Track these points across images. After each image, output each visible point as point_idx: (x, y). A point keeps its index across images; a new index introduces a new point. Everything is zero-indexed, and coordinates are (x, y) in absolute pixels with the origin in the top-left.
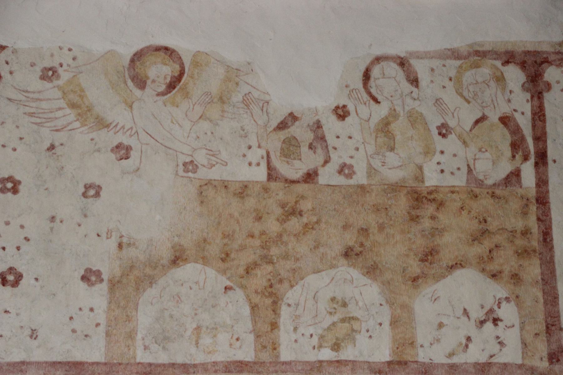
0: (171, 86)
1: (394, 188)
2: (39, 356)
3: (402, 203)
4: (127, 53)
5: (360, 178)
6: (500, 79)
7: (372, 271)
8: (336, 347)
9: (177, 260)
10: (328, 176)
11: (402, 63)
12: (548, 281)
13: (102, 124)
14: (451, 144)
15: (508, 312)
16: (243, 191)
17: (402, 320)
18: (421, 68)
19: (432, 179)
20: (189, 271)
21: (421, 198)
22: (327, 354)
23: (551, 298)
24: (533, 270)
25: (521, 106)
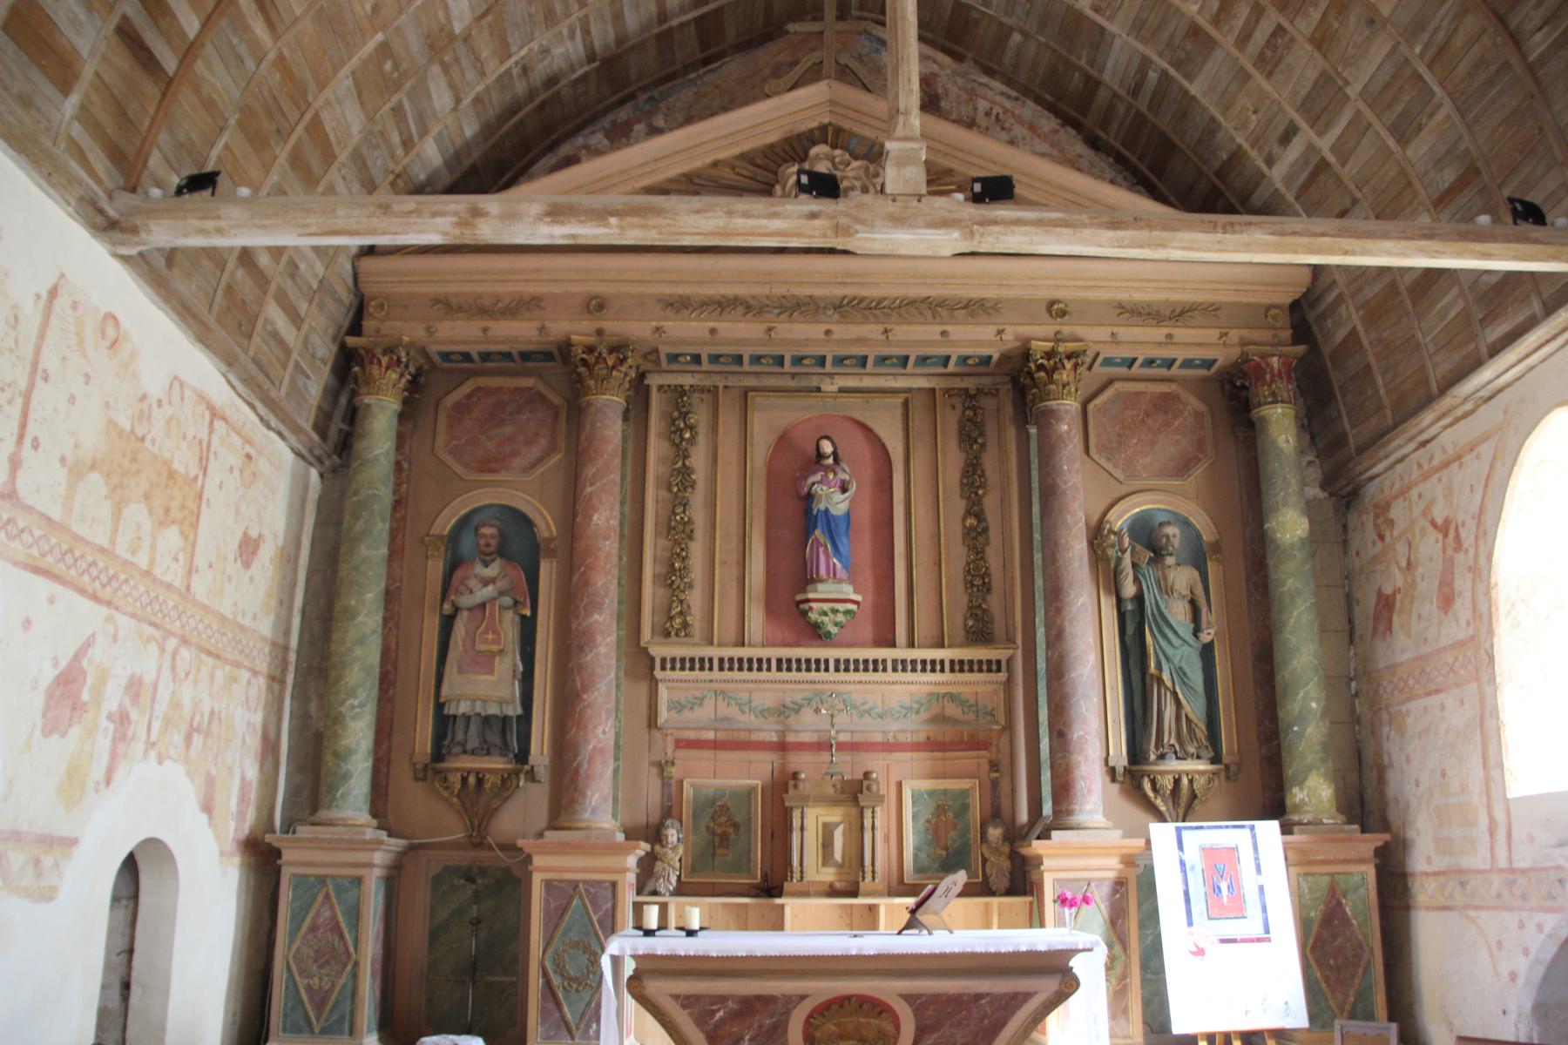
0: (114, 343)
1: (165, 463)
2: (39, 507)
3: (165, 474)
4: (103, 310)
5: (155, 450)
6: (203, 416)
7: (151, 511)
8: (133, 553)
9: (93, 467)
10: (148, 443)
11: (182, 386)
12: (194, 544)
13: (84, 355)
14: (184, 445)
15: (181, 556)
16: (121, 433)
17: (153, 548)
18: (188, 392)
19: (176, 466)
20: (95, 478)
21: (172, 474)
22: (128, 556)
23: (193, 555)
24: (191, 537)
25: (204, 435)
